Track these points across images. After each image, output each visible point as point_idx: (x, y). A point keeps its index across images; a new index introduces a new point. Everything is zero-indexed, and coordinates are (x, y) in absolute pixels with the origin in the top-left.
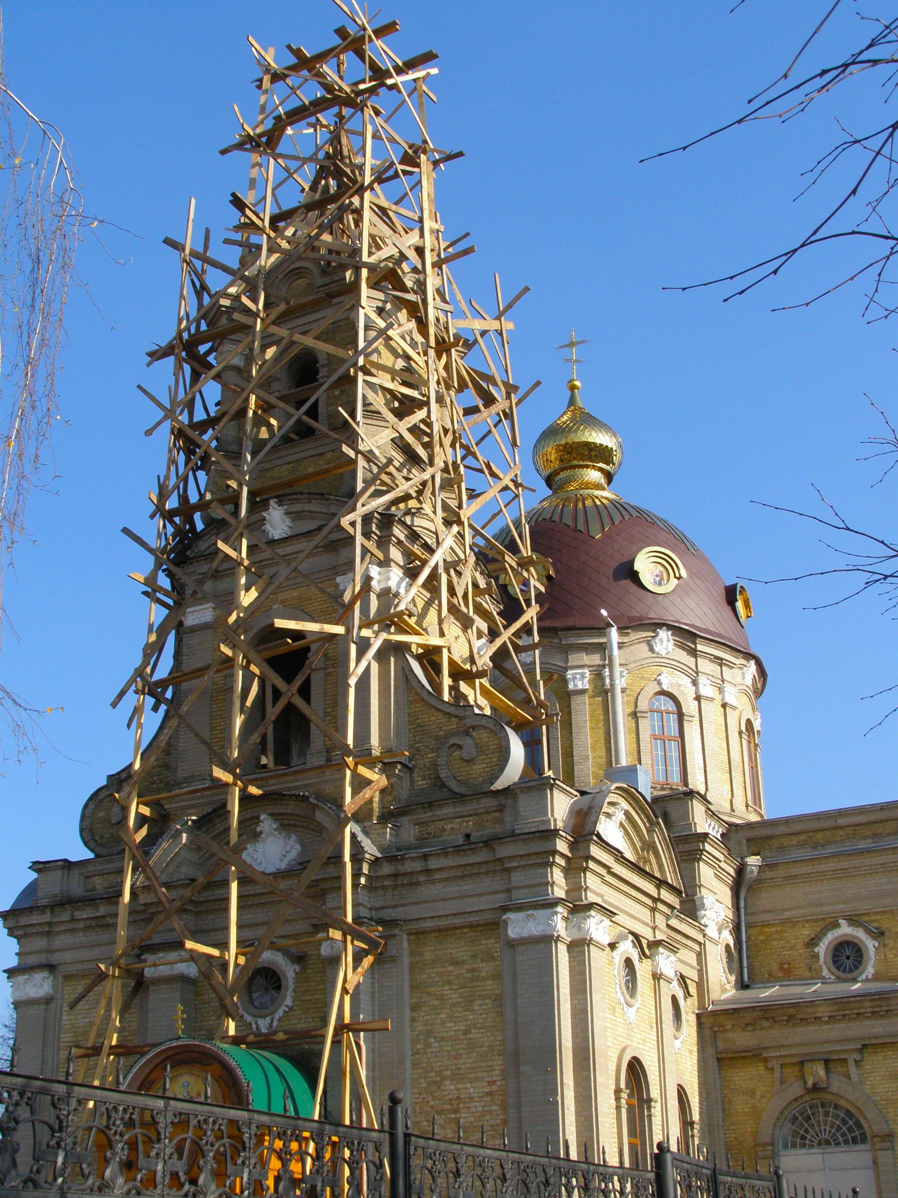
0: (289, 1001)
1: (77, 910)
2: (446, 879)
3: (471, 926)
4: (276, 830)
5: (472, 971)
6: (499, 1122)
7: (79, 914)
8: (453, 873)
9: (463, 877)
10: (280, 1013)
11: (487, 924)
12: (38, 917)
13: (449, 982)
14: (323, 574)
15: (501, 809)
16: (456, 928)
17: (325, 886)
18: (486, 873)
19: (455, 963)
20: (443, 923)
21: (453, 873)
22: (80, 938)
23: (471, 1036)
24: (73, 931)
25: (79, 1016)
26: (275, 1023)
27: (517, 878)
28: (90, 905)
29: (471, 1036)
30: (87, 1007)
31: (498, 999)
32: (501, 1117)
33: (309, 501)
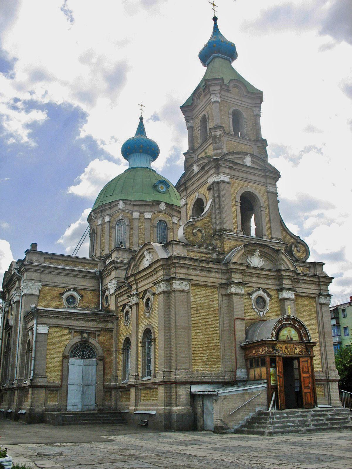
0: (268, 308)
1: (201, 263)
2: (305, 283)
3: (309, 297)
4: (258, 255)
5: (309, 309)
6: (318, 350)
7: (201, 265)
8: (307, 282)
9: (309, 283)
10: (265, 312)
11: (313, 297)
12: (188, 262)
13: (305, 311)
14: (262, 183)
15: (309, 267)
16: (306, 297)
17: (283, 277)
18: (314, 284)
19: (306, 306)
20: (304, 294)
21: (307, 282)
22: (198, 273)
23: (311, 326)
24: (196, 269)
25: (197, 300)
26: (264, 314)
27: (322, 287)
28: (206, 263)
29: (311, 326)
30: (200, 297)
31: (317, 318)
32: (319, 349)
33: (258, 160)
